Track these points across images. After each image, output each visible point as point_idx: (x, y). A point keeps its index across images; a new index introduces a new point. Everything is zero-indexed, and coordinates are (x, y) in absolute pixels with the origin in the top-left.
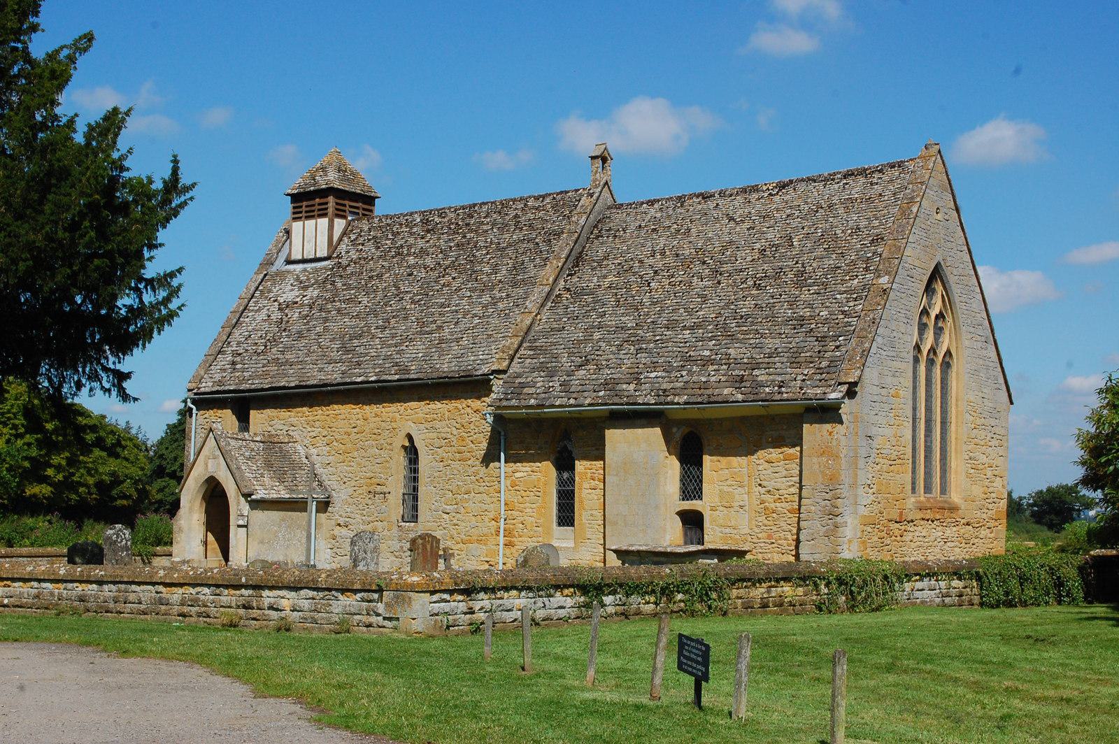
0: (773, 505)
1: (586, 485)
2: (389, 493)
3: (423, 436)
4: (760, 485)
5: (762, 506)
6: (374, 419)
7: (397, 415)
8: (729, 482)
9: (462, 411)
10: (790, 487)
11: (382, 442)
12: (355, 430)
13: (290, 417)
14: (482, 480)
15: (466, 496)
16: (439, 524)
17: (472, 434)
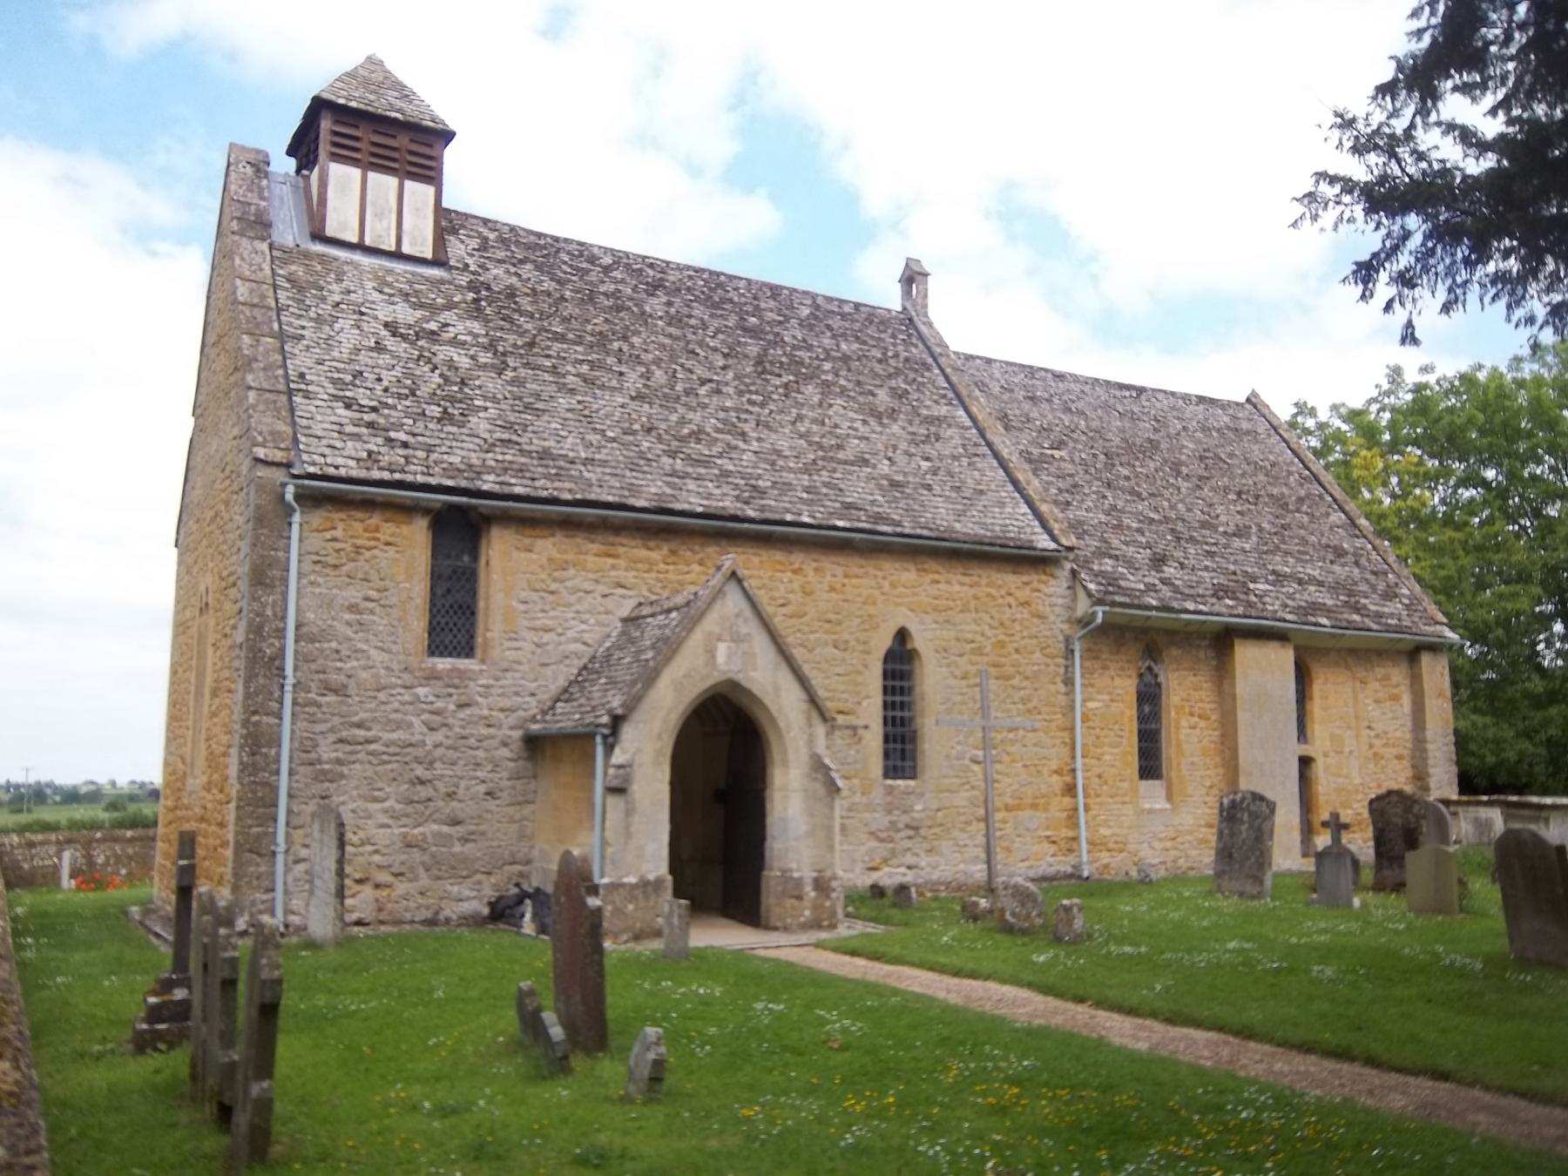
0: (1381, 750)
1: (1184, 723)
2: (866, 727)
3: (929, 635)
4: (1369, 727)
5: (1371, 752)
6: (826, 596)
7: (877, 593)
8: (1338, 724)
9: (1000, 601)
10: (1396, 730)
11: (846, 636)
12: (784, 610)
13: (613, 567)
14: (1035, 712)
15: (1011, 736)
16: (964, 780)
17: (1017, 638)
